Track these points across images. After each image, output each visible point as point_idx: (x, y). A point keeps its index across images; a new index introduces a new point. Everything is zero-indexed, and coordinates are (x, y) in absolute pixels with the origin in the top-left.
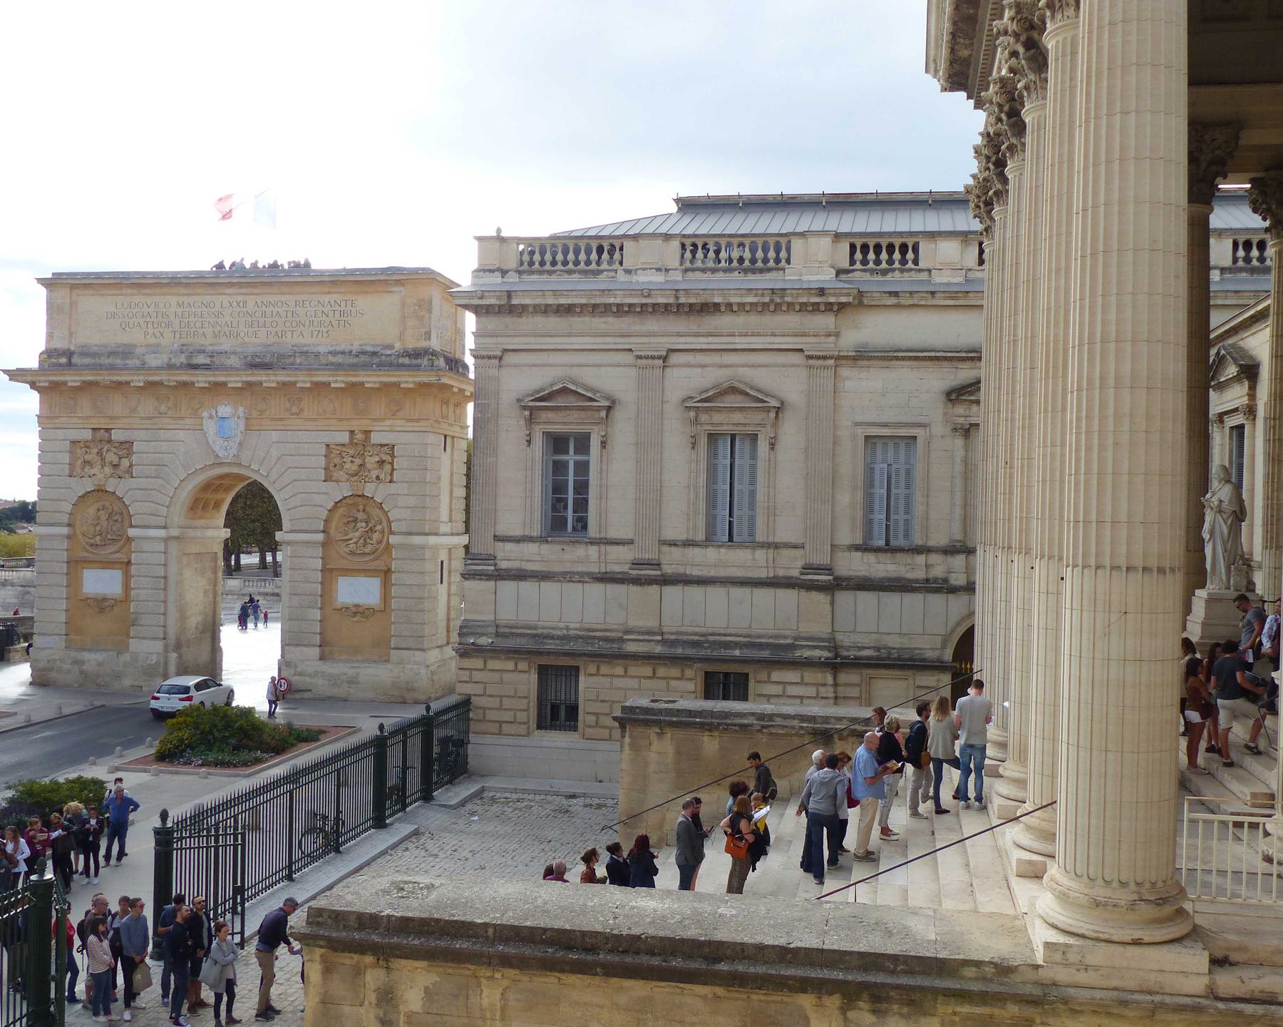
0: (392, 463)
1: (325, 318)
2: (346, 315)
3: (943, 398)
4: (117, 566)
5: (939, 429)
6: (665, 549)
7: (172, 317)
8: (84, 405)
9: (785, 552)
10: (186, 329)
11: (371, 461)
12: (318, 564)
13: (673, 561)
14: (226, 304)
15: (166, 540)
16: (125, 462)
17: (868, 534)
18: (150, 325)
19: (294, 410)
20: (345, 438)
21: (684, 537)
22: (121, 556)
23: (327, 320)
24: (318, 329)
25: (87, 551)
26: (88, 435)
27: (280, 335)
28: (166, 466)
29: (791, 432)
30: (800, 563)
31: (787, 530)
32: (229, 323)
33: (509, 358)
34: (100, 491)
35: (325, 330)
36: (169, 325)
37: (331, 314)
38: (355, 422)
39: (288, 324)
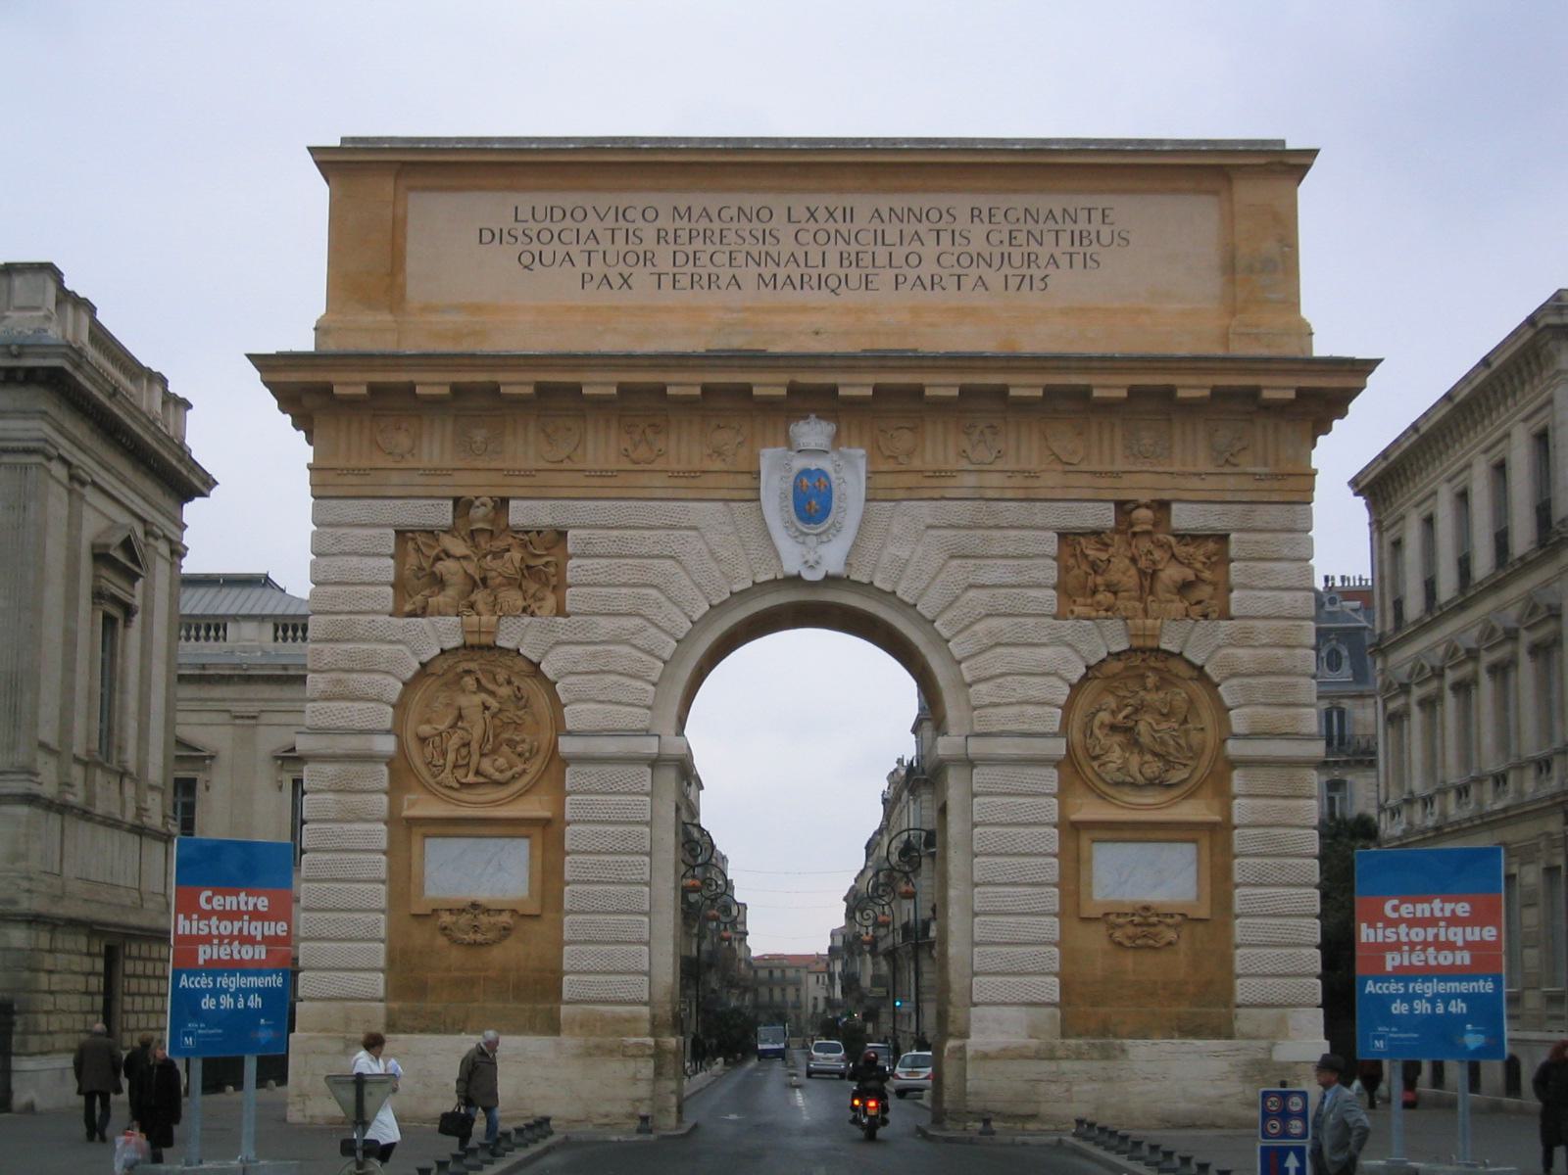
1: (1034, 247)
2: (1086, 242)
4: (523, 830)
7: (650, 242)
8: (435, 448)
10: (690, 268)
12: (1051, 808)
15: (655, 763)
18: (597, 258)
20: (1104, 516)
22: (533, 807)
23: (1044, 253)
24: (1024, 271)
27: (927, 282)
28: (655, 587)
32: (801, 260)
34: (480, 648)
35: (1038, 274)
36: (647, 258)
37: (1049, 238)
38: (1126, 481)
39: (945, 260)
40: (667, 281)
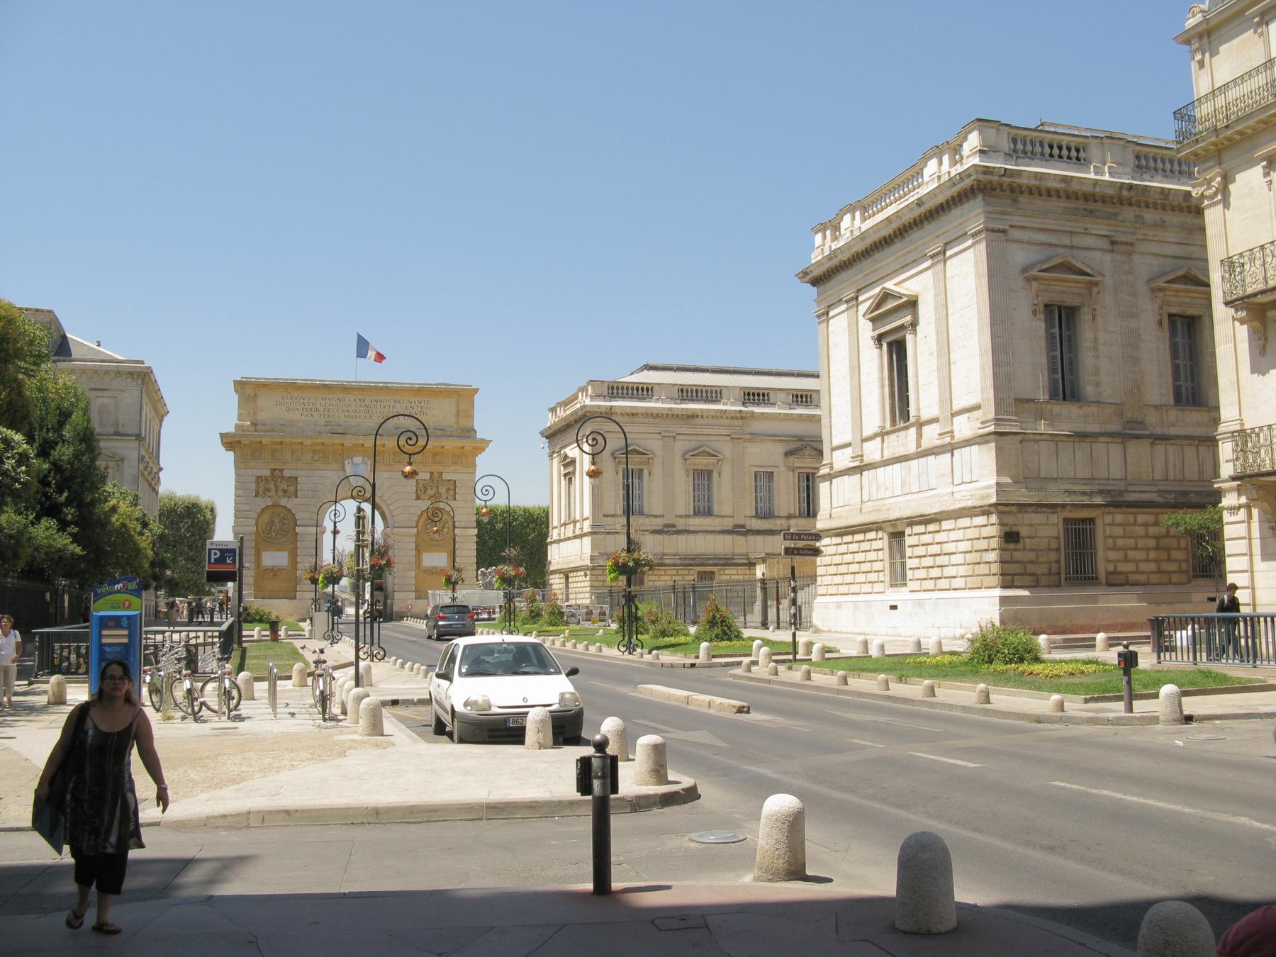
0: (455, 490)
3: (783, 456)
5: (782, 468)
6: (677, 519)
7: (319, 406)
9: (726, 519)
11: (443, 490)
13: (681, 524)
14: (352, 400)
16: (292, 489)
17: (756, 513)
19: (398, 460)
21: (684, 514)
25: (266, 541)
26: (268, 473)
29: (726, 469)
30: (732, 525)
31: (726, 510)
33: (678, 437)
34: (276, 505)
36: (317, 410)
37: (415, 408)
40: (322, 416)
